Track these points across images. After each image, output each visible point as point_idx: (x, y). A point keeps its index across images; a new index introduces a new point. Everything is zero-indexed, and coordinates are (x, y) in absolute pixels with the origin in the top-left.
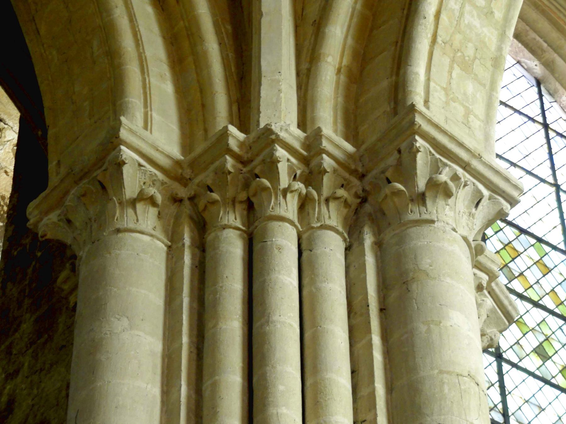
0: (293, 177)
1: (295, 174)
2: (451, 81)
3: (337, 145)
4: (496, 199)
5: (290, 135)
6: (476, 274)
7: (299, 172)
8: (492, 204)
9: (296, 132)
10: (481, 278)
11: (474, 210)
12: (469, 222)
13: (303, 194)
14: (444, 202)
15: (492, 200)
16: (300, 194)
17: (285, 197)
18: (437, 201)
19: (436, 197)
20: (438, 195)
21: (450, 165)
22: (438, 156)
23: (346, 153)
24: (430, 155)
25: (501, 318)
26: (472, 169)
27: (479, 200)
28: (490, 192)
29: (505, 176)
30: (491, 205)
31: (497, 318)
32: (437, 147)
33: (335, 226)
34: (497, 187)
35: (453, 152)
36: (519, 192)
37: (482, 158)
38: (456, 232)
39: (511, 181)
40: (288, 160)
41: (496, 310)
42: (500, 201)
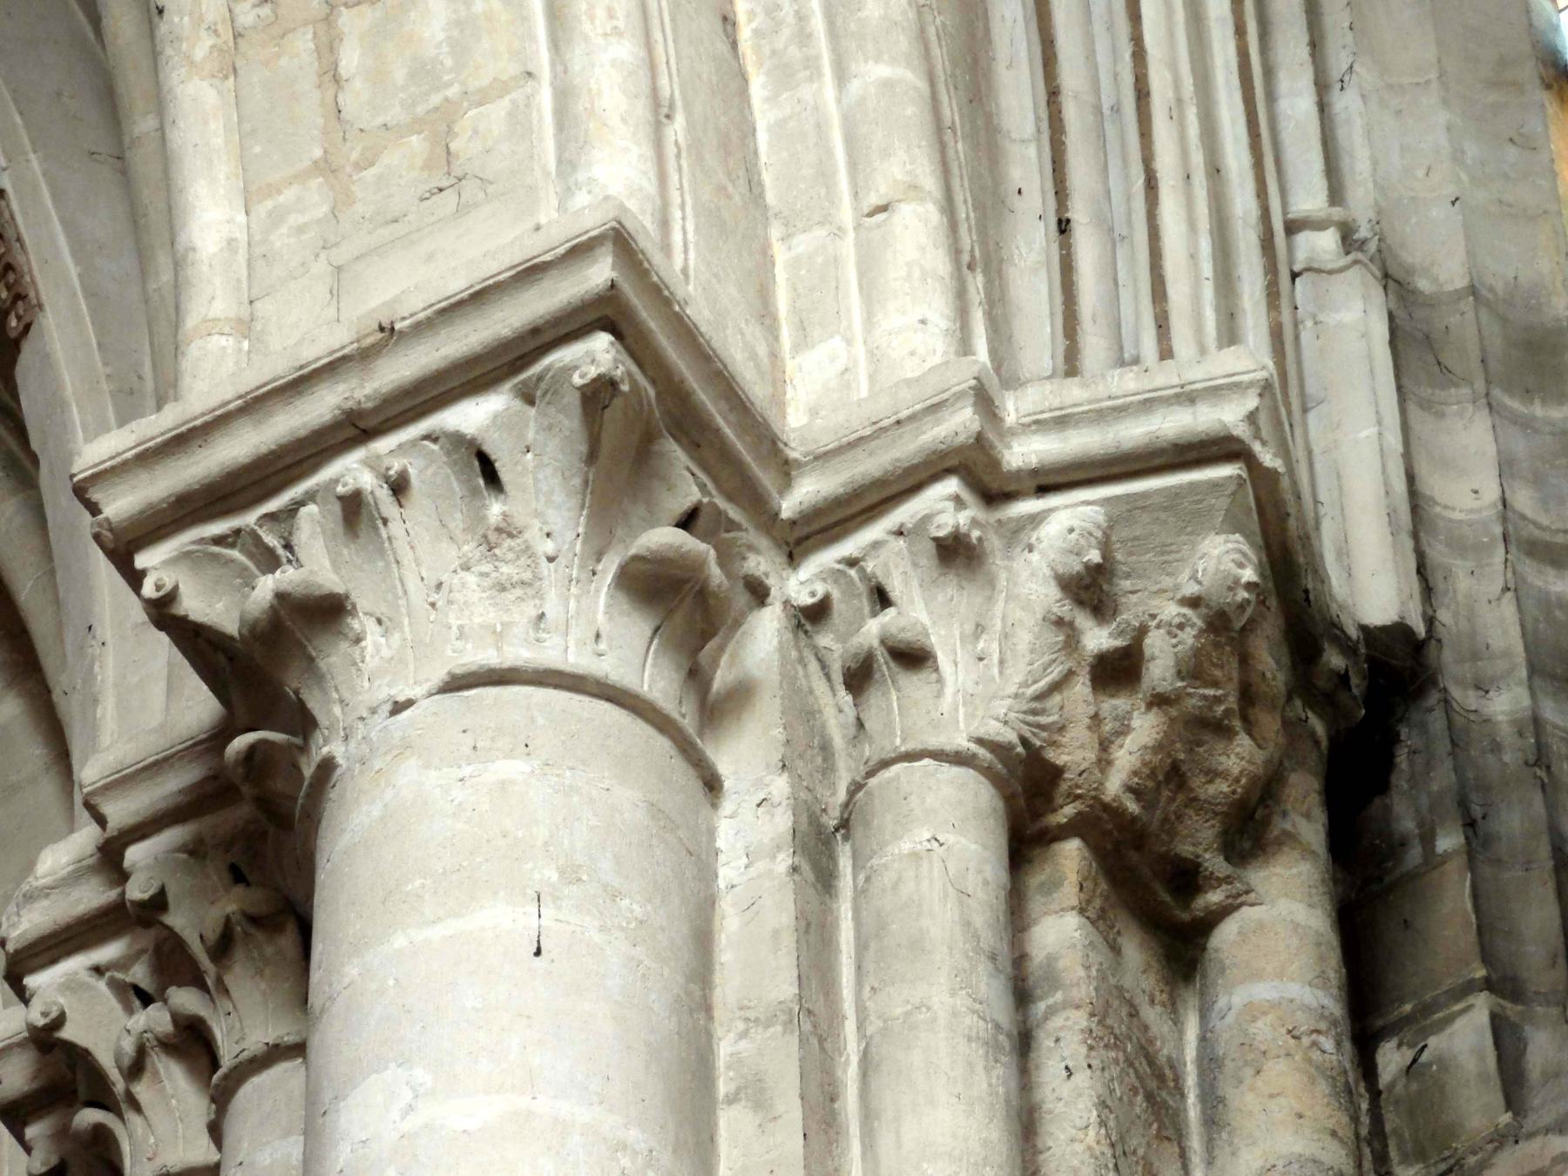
0: (137, 1003)
1: (132, 992)
2: (340, 99)
3: (156, 764)
4: (540, 378)
5: (47, 895)
6: (902, 525)
7: (140, 974)
8: (549, 403)
9: (64, 860)
10: (926, 519)
11: (495, 509)
12: (505, 569)
13: (167, 1036)
14: (344, 646)
15: (539, 393)
16: (168, 1046)
17: (136, 1106)
18: (322, 664)
19: (311, 659)
20: (310, 648)
21: (307, 493)
22: (249, 519)
23: (199, 748)
24: (233, 546)
25: (1175, 494)
26: (376, 410)
27: (476, 464)
28: (508, 385)
29: (513, 272)
30: (552, 410)
31: (1165, 509)
32: (224, 498)
33: (237, 1060)
34: (504, 346)
35: (272, 452)
36: (603, 249)
37: (397, 326)
38: (409, 703)
39: (547, 257)
40: (98, 970)
41: (1118, 498)
42: (558, 365)
